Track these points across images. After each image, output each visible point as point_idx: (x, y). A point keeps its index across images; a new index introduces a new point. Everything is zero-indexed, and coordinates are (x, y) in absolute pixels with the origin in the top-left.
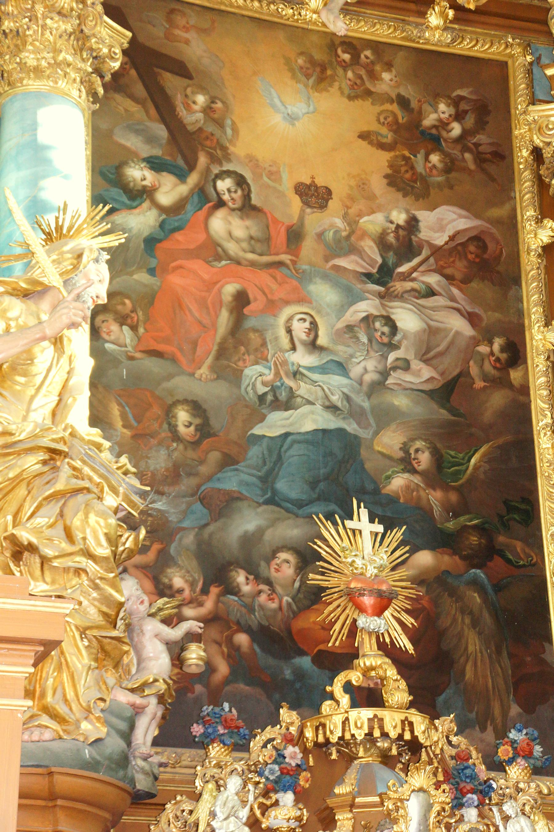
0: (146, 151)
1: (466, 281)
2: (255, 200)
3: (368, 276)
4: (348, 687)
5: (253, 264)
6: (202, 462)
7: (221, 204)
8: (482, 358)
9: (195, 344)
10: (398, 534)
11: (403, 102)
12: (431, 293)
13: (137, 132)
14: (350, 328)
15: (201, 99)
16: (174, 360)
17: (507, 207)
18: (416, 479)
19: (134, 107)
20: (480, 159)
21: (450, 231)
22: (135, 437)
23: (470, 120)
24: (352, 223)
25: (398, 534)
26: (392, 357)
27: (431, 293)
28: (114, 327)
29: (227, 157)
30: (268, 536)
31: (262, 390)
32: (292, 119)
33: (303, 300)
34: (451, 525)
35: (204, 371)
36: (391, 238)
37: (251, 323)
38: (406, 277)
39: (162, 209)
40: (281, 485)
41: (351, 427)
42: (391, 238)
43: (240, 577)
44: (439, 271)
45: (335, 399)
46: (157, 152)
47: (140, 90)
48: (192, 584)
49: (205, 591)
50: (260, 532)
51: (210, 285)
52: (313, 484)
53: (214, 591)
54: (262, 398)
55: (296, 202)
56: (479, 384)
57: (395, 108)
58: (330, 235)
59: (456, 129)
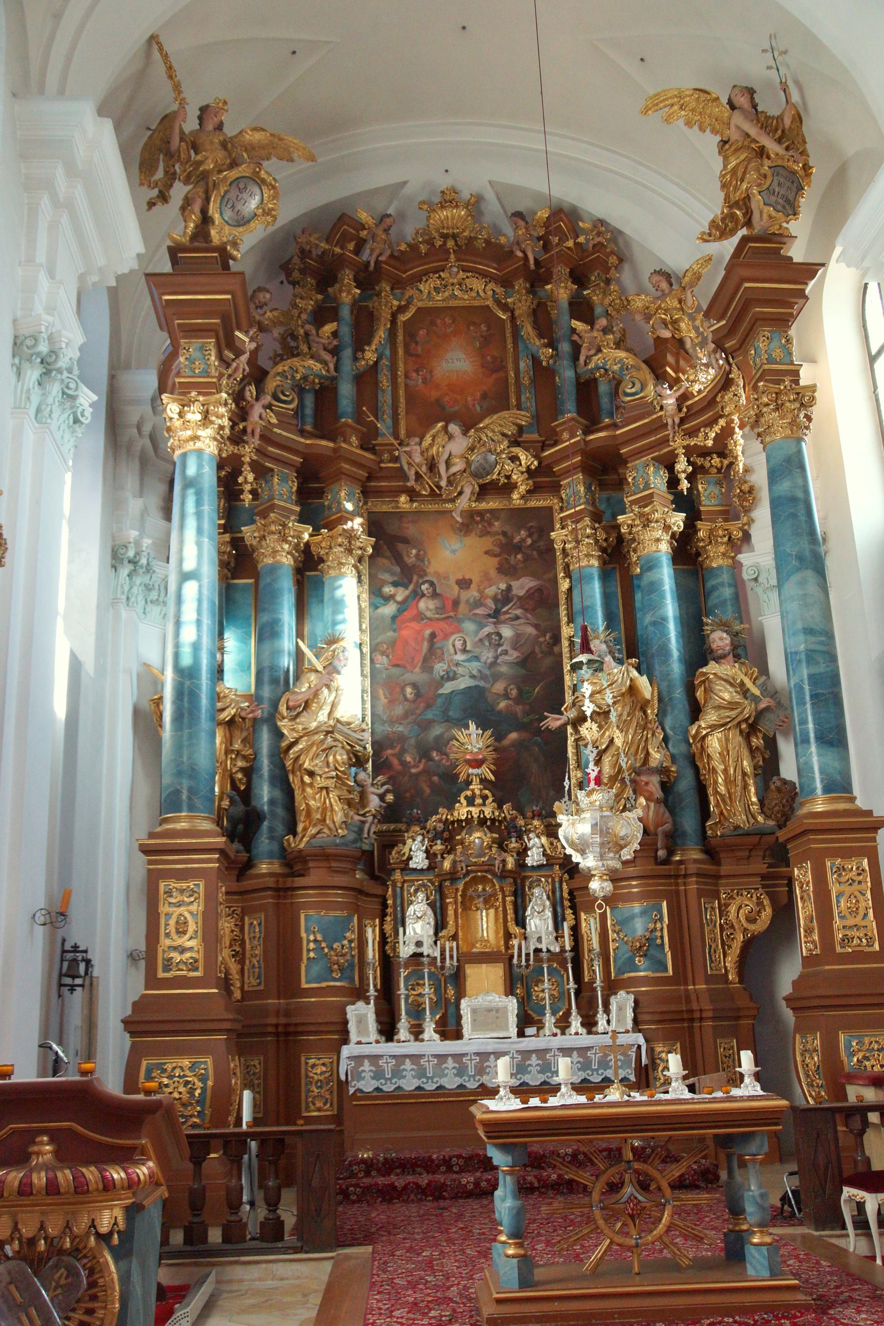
1: (534, 609)
2: (438, 591)
3: (489, 615)
4: (466, 798)
5: (438, 619)
6: (417, 708)
7: (423, 595)
8: (541, 643)
9: (413, 659)
10: (489, 733)
11: (504, 534)
12: (517, 618)
13: (387, 571)
14: (481, 640)
15: (414, 551)
16: (404, 667)
17: (552, 575)
18: (510, 702)
19: (385, 561)
20: (540, 553)
21: (527, 588)
22: (390, 702)
23: (535, 537)
25: (489, 733)
26: (499, 650)
27: (517, 618)
28: (380, 657)
29: (426, 574)
30: (445, 736)
31: (442, 673)
32: (454, 552)
33: (460, 631)
34: (525, 720)
35: (417, 670)
36: (499, 596)
37: (438, 645)
38: (506, 613)
39: (398, 603)
40: (451, 713)
41: (482, 684)
42: (499, 596)
43: (434, 754)
44: (522, 607)
45: (475, 672)
46: (396, 579)
47: (388, 554)
48: (414, 759)
49: (420, 761)
50: (442, 735)
51: (420, 632)
52: (465, 711)
53: (423, 761)
54: (442, 677)
55: (456, 588)
56: (539, 655)
57: (501, 537)
58: (471, 600)
59: (529, 541)
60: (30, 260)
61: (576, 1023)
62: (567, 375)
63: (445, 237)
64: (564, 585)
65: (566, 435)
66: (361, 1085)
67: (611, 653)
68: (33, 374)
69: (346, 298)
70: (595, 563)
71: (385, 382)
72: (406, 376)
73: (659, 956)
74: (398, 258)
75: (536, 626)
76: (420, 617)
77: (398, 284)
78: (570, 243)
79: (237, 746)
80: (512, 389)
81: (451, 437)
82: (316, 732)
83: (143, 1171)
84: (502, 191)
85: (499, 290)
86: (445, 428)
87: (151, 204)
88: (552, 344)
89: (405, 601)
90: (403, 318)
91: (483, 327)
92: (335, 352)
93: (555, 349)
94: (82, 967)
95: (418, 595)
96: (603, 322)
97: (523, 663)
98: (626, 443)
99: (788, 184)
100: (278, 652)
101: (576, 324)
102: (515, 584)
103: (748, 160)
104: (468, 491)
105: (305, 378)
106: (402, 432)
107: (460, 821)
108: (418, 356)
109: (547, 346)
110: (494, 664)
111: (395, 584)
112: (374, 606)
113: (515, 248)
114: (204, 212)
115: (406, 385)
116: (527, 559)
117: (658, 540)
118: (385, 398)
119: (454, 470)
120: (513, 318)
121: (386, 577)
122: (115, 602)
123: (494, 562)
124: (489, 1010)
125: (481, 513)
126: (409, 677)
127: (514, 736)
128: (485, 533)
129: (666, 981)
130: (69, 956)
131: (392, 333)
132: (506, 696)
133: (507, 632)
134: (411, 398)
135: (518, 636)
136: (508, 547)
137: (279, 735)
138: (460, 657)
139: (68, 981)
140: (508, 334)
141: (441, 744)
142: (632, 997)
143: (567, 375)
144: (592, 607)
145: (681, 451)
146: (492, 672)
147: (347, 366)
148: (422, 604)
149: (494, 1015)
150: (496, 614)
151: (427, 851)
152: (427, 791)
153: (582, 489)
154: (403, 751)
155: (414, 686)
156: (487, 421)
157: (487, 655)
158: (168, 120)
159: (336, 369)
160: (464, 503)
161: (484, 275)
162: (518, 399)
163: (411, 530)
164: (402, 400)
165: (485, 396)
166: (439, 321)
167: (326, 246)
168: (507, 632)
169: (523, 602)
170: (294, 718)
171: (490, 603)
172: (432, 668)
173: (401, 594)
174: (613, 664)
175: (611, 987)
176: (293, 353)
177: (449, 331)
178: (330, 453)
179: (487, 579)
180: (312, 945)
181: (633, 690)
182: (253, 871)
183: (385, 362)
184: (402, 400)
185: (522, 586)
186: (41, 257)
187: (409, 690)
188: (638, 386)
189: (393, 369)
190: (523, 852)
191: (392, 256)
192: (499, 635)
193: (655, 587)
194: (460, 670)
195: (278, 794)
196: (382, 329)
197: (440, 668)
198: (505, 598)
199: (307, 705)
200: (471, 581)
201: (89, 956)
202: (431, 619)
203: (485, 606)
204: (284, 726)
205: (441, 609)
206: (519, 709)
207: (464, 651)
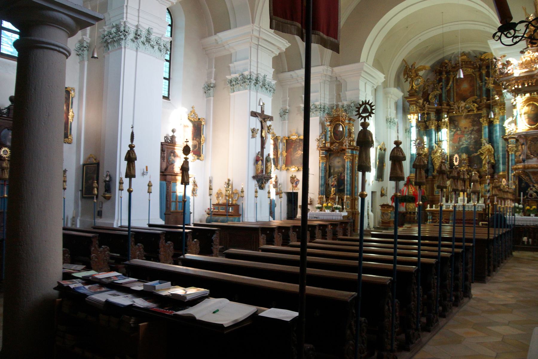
11: (473, 119)
12: (474, 134)
27: (474, 134)
55: (464, 129)
60: (387, 108)
61: (476, 202)
62: (484, 89)
67: (486, 142)
68: (389, 123)
70: (487, 125)
72: (456, 89)
75: (478, 135)
76: (458, 134)
77: (453, 72)
78: (485, 62)
82: (437, 157)
83: (391, 209)
84: (474, 51)
85: (473, 70)
87: (405, 82)
88: (482, 82)
89: (455, 131)
92: (441, 89)
95: (457, 130)
100: (432, 143)
101: (486, 78)
102: (474, 128)
104: (465, 112)
105: (436, 94)
106: (455, 101)
109: (481, 82)
110: (470, 142)
111: (454, 129)
112: (450, 133)
113: (475, 64)
114: (412, 84)
115: (456, 92)
116: (477, 123)
117: (496, 122)
118: (452, 94)
120: (476, 76)
121: (452, 127)
122: (406, 138)
123: (471, 124)
126: (455, 145)
131: (453, 81)
132: (472, 148)
133: (473, 136)
134: (457, 94)
135: (475, 137)
136: (474, 121)
137: (431, 157)
138: (464, 141)
140: (475, 79)
143: (484, 89)
153: (485, 111)
155: (457, 146)
156: (469, 99)
157: (469, 141)
160: (465, 114)
163: (456, 119)
165: (470, 92)
167: (439, 68)
168: (473, 136)
169: (476, 131)
170: (434, 155)
171: (470, 131)
173: (455, 130)
175: (482, 197)
179: (469, 127)
182: (428, 178)
183: (452, 87)
185: (476, 128)
186: (389, 107)
189: (453, 88)
192: (471, 137)
194: (464, 143)
195: (432, 166)
197: (461, 143)
198: (473, 130)
199: (436, 152)
204: (432, 155)
205: (461, 133)
207: (465, 140)
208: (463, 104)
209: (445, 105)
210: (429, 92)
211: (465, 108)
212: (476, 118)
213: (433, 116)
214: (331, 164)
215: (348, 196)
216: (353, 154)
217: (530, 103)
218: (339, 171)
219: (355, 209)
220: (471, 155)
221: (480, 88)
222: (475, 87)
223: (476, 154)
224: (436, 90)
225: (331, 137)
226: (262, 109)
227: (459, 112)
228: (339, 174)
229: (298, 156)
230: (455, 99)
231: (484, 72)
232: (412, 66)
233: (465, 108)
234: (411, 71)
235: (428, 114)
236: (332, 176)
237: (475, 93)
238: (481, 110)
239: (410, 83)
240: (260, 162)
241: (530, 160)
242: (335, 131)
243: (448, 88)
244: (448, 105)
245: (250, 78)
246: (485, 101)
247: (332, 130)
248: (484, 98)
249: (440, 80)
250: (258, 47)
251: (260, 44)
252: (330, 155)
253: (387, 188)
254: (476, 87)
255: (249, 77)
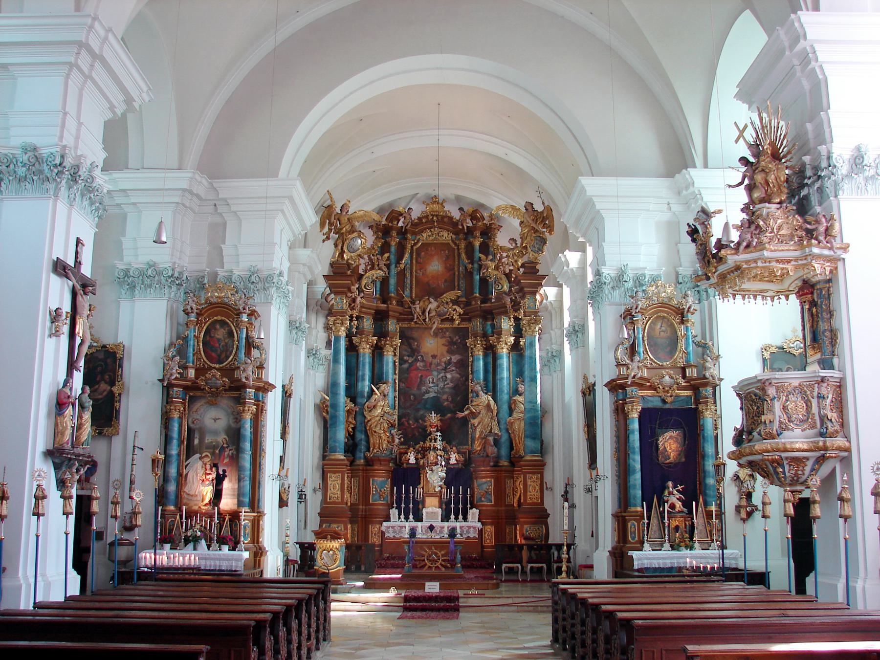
0: (407, 354)
11: (450, 337)
12: (453, 371)
19: (405, 347)
24: (440, 360)
27: (453, 371)
29: (420, 352)
32: (431, 344)
41: (439, 395)
43: (420, 421)
45: (436, 391)
47: (406, 344)
55: (431, 358)
59: (459, 341)
62: (477, 278)
63: (433, 215)
64: (471, 359)
65: (473, 303)
66: (389, 535)
67: (482, 390)
69: (393, 243)
71: (408, 275)
73: (489, 497)
74: (414, 225)
75: (460, 374)
76: (417, 369)
77: (415, 234)
78: (480, 224)
79: (350, 419)
80: (456, 278)
81: (430, 302)
82: (377, 416)
85: (454, 236)
86: (429, 299)
88: (472, 263)
89: (412, 362)
90: (415, 248)
91: (447, 252)
92: (388, 266)
93: (473, 265)
94: (304, 496)
95: (417, 360)
96: (491, 257)
97: (454, 388)
98: (495, 309)
99: (540, 243)
102: (453, 357)
103: (529, 231)
105: (377, 278)
107: (426, 447)
108: (420, 263)
110: (444, 388)
111: (408, 356)
113: (460, 223)
114: (342, 248)
115: (416, 276)
117: (503, 348)
119: (431, 315)
121: (404, 353)
124: (432, 513)
125: (442, 329)
127: (449, 415)
128: (443, 337)
129: (492, 506)
130: (300, 493)
132: (447, 400)
135: (453, 377)
136: (451, 343)
138: (431, 385)
139: (300, 500)
141: (423, 418)
142: (478, 511)
144: (480, 370)
145: (512, 316)
146: (442, 391)
147: (394, 271)
148: (418, 364)
149: (434, 514)
150: (445, 369)
151: (415, 457)
152: (417, 434)
154: (409, 419)
157: (441, 385)
158: (330, 208)
159: (388, 274)
161: (448, 230)
162: (459, 285)
163: (415, 335)
164: (414, 282)
165: (446, 281)
166: (429, 249)
172: (421, 389)
174: (483, 394)
176: (372, 268)
177: (433, 253)
178: (385, 309)
180: (374, 489)
181: (488, 405)
182: (356, 463)
184: (414, 282)
185: (455, 358)
187: (412, 397)
188: (500, 287)
190: (449, 459)
191: (412, 224)
192: (446, 377)
193: (501, 365)
194: (431, 390)
196: (407, 254)
198: (449, 362)
200: (437, 356)
201: (306, 493)
202: (421, 370)
203: (441, 365)
206: (451, 405)
207: (433, 382)
208: (433, 305)
209: (394, 302)
210: (361, 272)
211: (439, 315)
212: (457, 337)
213: (368, 324)
214: (193, 423)
215: (247, 509)
216: (259, 401)
217: (659, 314)
218: (218, 442)
219: (258, 542)
220: (446, 415)
221: (469, 275)
222: (457, 273)
223: (461, 415)
224: (377, 268)
225: (196, 353)
226: (76, 257)
227: (424, 320)
228: (217, 451)
229: (100, 397)
230: (414, 291)
231: (477, 244)
232: (342, 207)
233: (439, 315)
234: (339, 219)
235: (358, 318)
236: (198, 455)
237: (456, 284)
238: (469, 320)
239: (336, 245)
240: (69, 411)
241: (786, 433)
242: (208, 338)
243: (402, 266)
244: (401, 303)
245: (60, 164)
246: (479, 302)
247: (202, 334)
248: (476, 297)
249: (385, 248)
250: (85, 82)
251: (94, 75)
252: (192, 400)
253: (289, 487)
254: (459, 272)
255: (58, 162)
